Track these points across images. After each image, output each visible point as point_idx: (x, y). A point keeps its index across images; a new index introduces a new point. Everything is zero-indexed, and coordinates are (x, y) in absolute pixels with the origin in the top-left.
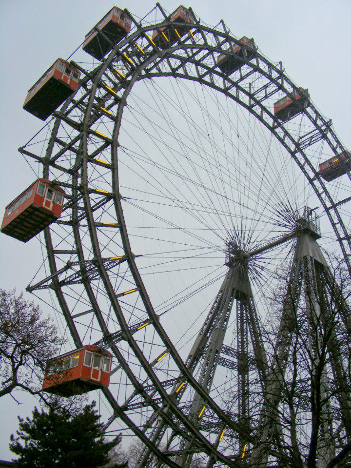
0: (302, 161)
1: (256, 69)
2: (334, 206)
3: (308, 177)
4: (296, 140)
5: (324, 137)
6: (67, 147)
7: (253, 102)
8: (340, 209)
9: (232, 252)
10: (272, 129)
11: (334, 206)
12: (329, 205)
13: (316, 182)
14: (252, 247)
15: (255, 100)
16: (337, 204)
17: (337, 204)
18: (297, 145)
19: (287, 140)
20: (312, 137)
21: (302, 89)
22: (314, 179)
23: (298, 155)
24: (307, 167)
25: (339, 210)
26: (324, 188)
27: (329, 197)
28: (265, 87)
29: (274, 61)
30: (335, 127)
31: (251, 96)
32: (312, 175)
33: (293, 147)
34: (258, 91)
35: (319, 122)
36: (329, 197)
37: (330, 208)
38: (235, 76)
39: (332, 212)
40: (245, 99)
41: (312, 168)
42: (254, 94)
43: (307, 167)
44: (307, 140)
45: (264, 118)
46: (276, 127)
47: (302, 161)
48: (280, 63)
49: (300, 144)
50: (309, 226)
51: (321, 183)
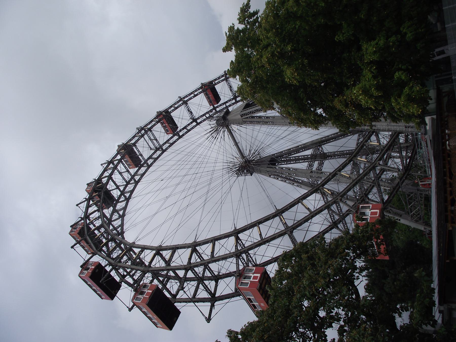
0: (167, 145)
1: (110, 177)
2: (195, 120)
3: (178, 139)
4: (152, 151)
5: (150, 129)
7: (133, 181)
8: (196, 115)
9: (243, 172)
12: (194, 124)
13: (181, 134)
14: (238, 156)
15: (131, 180)
18: (157, 149)
19: (155, 156)
21: (118, 149)
23: (164, 148)
24: (171, 141)
26: (183, 129)
27: (189, 125)
28: (120, 173)
29: (101, 169)
30: (142, 125)
31: (128, 183)
32: (176, 137)
33: (159, 153)
36: (189, 125)
38: (116, 193)
39: (199, 121)
40: (130, 188)
41: (171, 138)
42: (126, 181)
43: (171, 141)
47: (167, 145)
48: (102, 165)
49: (156, 148)
50: (221, 117)
51: (180, 131)
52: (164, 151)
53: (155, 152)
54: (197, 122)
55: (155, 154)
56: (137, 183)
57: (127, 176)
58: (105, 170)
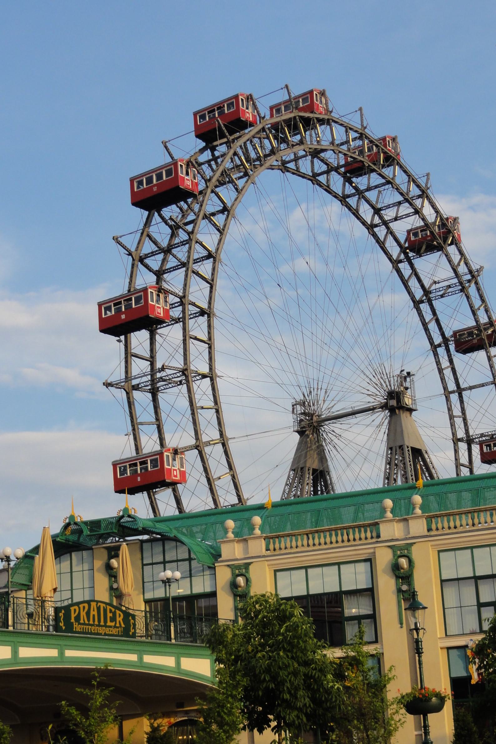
6: (191, 261)
10: (395, 263)
11: (460, 391)
12: (452, 386)
16: (465, 389)
17: (465, 389)
18: (427, 292)
19: (413, 283)
20: (449, 287)
22: (439, 345)
25: (465, 399)
31: (377, 211)
33: (419, 294)
34: (388, 207)
35: (462, 269)
37: (453, 392)
39: (454, 398)
40: (366, 212)
44: (441, 289)
45: (387, 245)
46: (401, 261)
47: (428, 316)
48: (428, 175)
52: (417, 304)
53: (423, 286)
54: (453, 392)
55: (418, 285)
56: (371, 227)
57: (389, 214)
58: (411, 179)
